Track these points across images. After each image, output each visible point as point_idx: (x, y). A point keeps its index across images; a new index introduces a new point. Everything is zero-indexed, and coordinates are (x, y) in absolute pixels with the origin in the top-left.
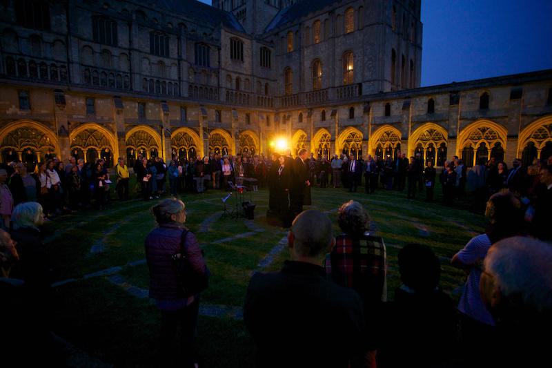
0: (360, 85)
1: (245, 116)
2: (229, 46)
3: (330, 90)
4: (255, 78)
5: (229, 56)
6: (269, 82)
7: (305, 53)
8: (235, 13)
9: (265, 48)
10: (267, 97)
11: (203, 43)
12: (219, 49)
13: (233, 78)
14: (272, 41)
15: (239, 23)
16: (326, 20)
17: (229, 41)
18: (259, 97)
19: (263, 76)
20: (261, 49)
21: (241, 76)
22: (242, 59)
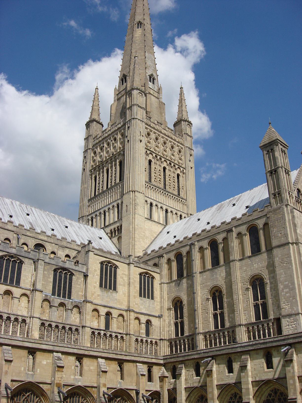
0: (278, 321)
2: (99, 272)
5: (98, 283)
6: (151, 318)
9: (147, 273)
10: (149, 340)
11: (64, 269)
12: (86, 276)
13: (101, 313)
19: (144, 311)
20: (141, 274)
21: (111, 310)
22: (115, 289)
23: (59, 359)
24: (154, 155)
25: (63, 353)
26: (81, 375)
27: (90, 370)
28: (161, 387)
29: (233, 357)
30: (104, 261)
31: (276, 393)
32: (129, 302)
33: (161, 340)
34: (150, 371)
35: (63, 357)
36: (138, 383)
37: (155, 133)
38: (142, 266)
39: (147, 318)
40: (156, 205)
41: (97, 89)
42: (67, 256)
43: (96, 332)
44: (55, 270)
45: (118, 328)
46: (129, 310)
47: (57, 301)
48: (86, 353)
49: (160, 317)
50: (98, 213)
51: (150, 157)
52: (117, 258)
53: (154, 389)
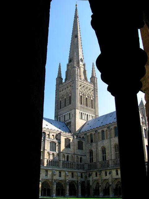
1: (71, 174)
3: (110, 161)
4: (76, 155)
7: (99, 143)
8: (66, 123)
9: (80, 141)
10: (81, 164)
11: (53, 142)
14: (83, 137)
15: (68, 128)
16: (106, 130)
17: (64, 140)
18: (77, 164)
19: (79, 154)
20: (78, 142)
21: (68, 155)
22: (70, 147)
23: (54, 172)
24: (83, 93)
25: (55, 170)
26: (61, 177)
27: (63, 175)
28: (85, 180)
29: (107, 171)
30: (66, 138)
31: (119, 182)
32: (74, 151)
33: (85, 163)
34: (81, 174)
35: (55, 171)
36: (78, 179)
37: (83, 85)
38: (79, 138)
39: (81, 156)
40: (84, 113)
41: (60, 64)
42: (53, 135)
43: (64, 162)
44: (50, 143)
45: (71, 160)
46: (74, 154)
47: (51, 152)
48: (62, 170)
49: (85, 155)
50: (62, 116)
51: (81, 95)
52: (70, 137)
53: (83, 180)
